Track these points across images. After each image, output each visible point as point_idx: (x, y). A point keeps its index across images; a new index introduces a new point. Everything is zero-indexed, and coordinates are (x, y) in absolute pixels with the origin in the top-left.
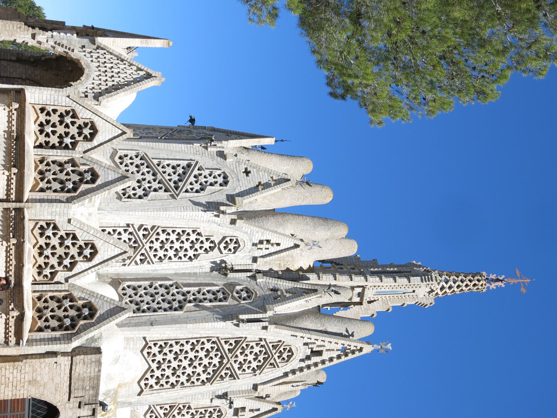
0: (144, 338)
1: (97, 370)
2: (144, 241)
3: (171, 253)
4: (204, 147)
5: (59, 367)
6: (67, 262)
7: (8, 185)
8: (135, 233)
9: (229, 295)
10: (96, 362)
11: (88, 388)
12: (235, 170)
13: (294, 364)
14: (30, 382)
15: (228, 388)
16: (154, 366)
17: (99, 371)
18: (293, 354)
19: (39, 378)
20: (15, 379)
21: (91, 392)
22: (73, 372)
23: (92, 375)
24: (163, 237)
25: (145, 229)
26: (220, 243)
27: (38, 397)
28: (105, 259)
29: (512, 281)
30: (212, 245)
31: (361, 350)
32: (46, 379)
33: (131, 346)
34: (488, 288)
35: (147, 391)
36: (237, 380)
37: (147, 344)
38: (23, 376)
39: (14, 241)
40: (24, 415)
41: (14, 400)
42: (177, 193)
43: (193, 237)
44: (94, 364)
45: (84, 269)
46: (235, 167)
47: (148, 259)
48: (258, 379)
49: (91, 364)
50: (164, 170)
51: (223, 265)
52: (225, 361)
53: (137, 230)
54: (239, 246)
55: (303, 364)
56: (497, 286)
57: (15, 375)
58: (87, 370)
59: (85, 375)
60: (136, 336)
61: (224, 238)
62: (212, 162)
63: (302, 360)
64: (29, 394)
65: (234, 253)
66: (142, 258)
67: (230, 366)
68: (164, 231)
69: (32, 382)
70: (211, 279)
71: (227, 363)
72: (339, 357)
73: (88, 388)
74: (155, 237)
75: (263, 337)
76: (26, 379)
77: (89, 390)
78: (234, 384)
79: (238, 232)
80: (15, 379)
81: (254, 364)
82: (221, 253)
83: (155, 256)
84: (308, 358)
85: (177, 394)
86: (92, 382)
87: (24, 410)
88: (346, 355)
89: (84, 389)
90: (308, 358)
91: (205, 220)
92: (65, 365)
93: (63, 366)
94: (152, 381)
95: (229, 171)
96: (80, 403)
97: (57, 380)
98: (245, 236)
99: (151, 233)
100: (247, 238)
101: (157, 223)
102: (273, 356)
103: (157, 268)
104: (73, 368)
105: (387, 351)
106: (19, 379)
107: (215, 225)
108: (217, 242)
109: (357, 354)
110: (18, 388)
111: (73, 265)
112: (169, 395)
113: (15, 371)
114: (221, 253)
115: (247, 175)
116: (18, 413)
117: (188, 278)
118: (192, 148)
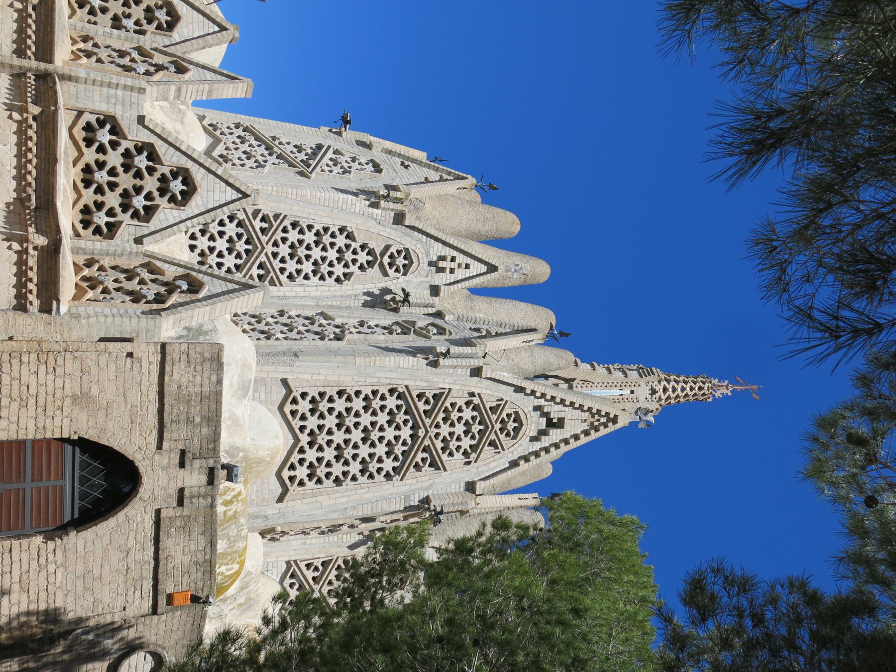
0: (285, 382)
1: (214, 378)
2: (264, 239)
3: (307, 267)
4: (335, 133)
5: (136, 365)
6: (139, 202)
7: (19, 155)
8: (248, 223)
10: (211, 360)
11: (198, 420)
13: (523, 446)
14: (75, 399)
15: (428, 488)
16: (304, 439)
17: (220, 382)
18: (521, 425)
19: (95, 391)
20: (42, 390)
21: (205, 431)
22: (167, 378)
23: (206, 389)
24: (293, 236)
25: (263, 219)
26: (383, 254)
27: (92, 435)
28: (210, 206)
29: (739, 388)
30: (370, 258)
31: (615, 420)
32: (110, 392)
33: (263, 395)
34: (714, 396)
35: (294, 488)
36: (444, 474)
37: (289, 390)
38: (59, 382)
39: (35, 110)
40: (62, 488)
41: (41, 440)
42: (310, 170)
43: (341, 241)
44: (208, 364)
45: (172, 222)
47: (272, 274)
48: (473, 473)
49: (202, 363)
51: (388, 297)
52: (421, 432)
53: (251, 217)
54: (412, 262)
55: (537, 446)
56: (722, 394)
57: (42, 380)
58: (194, 377)
59: (191, 389)
60: (271, 375)
61: (387, 247)
63: (533, 439)
64: (74, 428)
65: (405, 274)
66: (262, 272)
67: (430, 443)
68: (294, 225)
69: (82, 399)
71: (425, 437)
72: (586, 433)
73: (198, 420)
74: (279, 235)
75: (476, 391)
76: (68, 391)
77: (200, 425)
78: (438, 480)
79: (408, 238)
80: (42, 390)
81: (466, 443)
82: (385, 274)
83: (282, 270)
84: (543, 433)
85: (345, 499)
86: (206, 407)
87: (63, 477)
88: (597, 430)
89: (189, 421)
90: (543, 433)
91: (357, 212)
92: (150, 363)
93: (145, 364)
94: (302, 472)
96: (183, 453)
97: (134, 397)
98: (419, 246)
99: (275, 225)
100: (423, 251)
101: (282, 209)
102: (493, 427)
103: (287, 294)
104: (168, 369)
105: (648, 424)
106: (50, 389)
107: (374, 222)
108: (378, 252)
109: (612, 428)
110: (49, 413)
111: (150, 211)
112: (333, 501)
113: (43, 368)
114: (385, 274)
116: (50, 484)
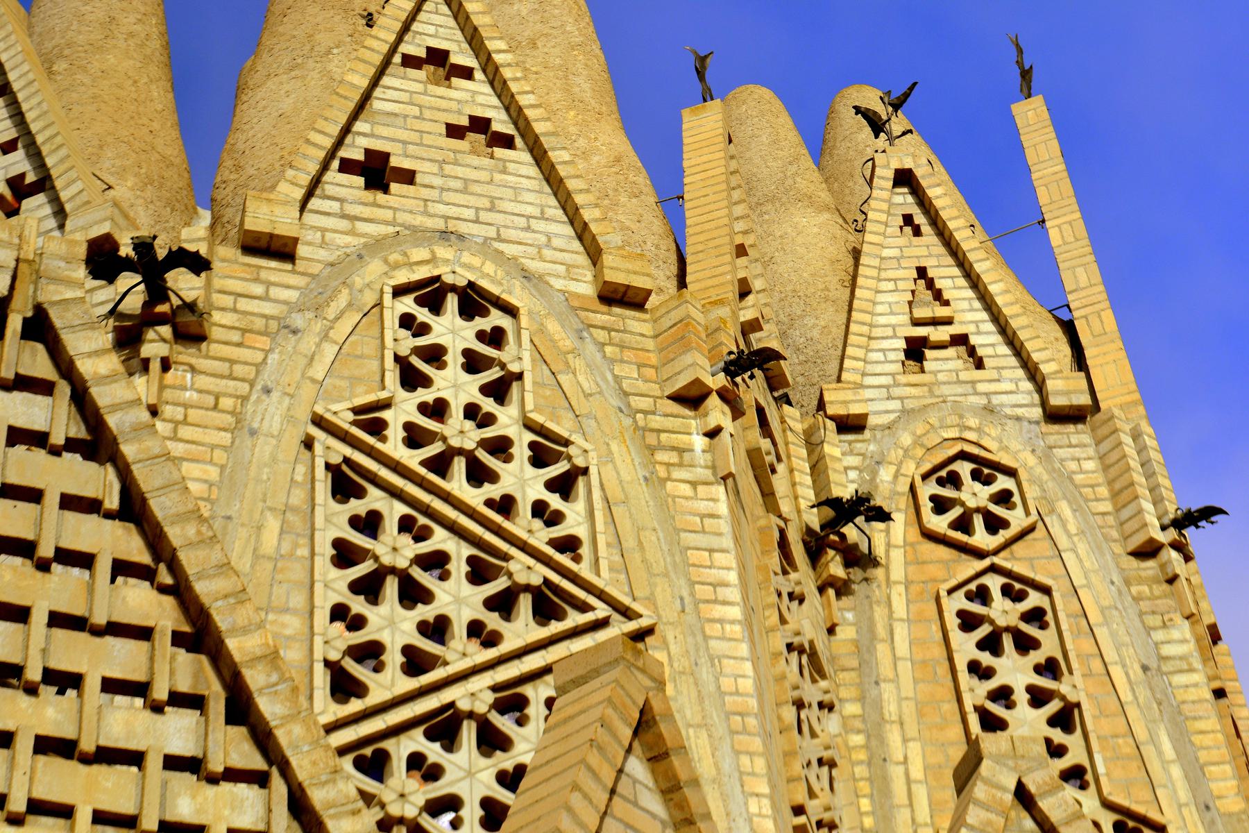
9: (993, 569)
12: (362, 227)
42: (602, 611)
46: (344, 224)
50: (393, 658)
62: (308, 343)
70: (882, 650)
95: (374, 268)
115: (408, 177)
117: (897, 772)
118: (185, 432)
